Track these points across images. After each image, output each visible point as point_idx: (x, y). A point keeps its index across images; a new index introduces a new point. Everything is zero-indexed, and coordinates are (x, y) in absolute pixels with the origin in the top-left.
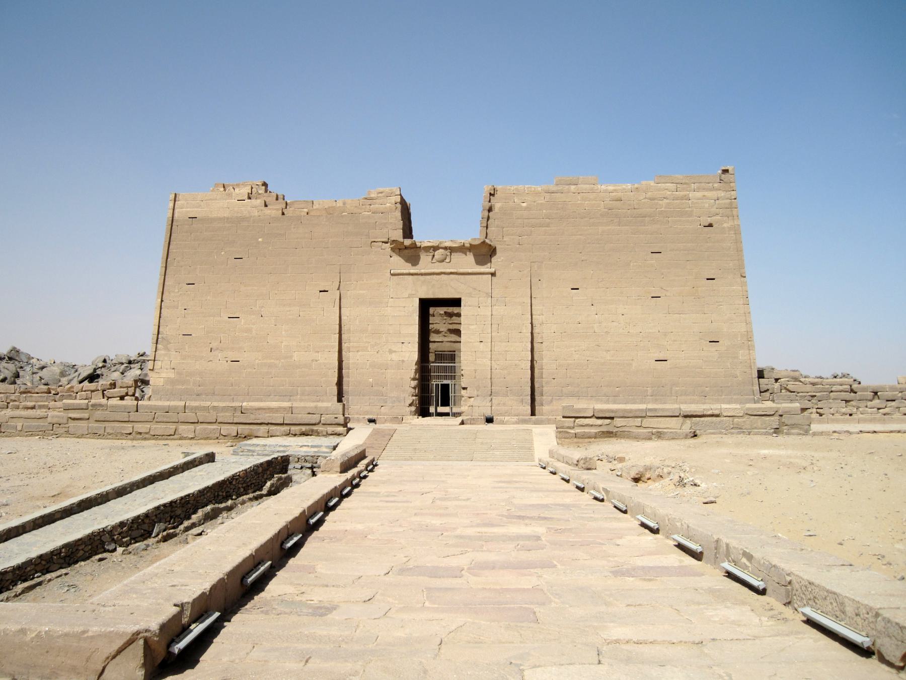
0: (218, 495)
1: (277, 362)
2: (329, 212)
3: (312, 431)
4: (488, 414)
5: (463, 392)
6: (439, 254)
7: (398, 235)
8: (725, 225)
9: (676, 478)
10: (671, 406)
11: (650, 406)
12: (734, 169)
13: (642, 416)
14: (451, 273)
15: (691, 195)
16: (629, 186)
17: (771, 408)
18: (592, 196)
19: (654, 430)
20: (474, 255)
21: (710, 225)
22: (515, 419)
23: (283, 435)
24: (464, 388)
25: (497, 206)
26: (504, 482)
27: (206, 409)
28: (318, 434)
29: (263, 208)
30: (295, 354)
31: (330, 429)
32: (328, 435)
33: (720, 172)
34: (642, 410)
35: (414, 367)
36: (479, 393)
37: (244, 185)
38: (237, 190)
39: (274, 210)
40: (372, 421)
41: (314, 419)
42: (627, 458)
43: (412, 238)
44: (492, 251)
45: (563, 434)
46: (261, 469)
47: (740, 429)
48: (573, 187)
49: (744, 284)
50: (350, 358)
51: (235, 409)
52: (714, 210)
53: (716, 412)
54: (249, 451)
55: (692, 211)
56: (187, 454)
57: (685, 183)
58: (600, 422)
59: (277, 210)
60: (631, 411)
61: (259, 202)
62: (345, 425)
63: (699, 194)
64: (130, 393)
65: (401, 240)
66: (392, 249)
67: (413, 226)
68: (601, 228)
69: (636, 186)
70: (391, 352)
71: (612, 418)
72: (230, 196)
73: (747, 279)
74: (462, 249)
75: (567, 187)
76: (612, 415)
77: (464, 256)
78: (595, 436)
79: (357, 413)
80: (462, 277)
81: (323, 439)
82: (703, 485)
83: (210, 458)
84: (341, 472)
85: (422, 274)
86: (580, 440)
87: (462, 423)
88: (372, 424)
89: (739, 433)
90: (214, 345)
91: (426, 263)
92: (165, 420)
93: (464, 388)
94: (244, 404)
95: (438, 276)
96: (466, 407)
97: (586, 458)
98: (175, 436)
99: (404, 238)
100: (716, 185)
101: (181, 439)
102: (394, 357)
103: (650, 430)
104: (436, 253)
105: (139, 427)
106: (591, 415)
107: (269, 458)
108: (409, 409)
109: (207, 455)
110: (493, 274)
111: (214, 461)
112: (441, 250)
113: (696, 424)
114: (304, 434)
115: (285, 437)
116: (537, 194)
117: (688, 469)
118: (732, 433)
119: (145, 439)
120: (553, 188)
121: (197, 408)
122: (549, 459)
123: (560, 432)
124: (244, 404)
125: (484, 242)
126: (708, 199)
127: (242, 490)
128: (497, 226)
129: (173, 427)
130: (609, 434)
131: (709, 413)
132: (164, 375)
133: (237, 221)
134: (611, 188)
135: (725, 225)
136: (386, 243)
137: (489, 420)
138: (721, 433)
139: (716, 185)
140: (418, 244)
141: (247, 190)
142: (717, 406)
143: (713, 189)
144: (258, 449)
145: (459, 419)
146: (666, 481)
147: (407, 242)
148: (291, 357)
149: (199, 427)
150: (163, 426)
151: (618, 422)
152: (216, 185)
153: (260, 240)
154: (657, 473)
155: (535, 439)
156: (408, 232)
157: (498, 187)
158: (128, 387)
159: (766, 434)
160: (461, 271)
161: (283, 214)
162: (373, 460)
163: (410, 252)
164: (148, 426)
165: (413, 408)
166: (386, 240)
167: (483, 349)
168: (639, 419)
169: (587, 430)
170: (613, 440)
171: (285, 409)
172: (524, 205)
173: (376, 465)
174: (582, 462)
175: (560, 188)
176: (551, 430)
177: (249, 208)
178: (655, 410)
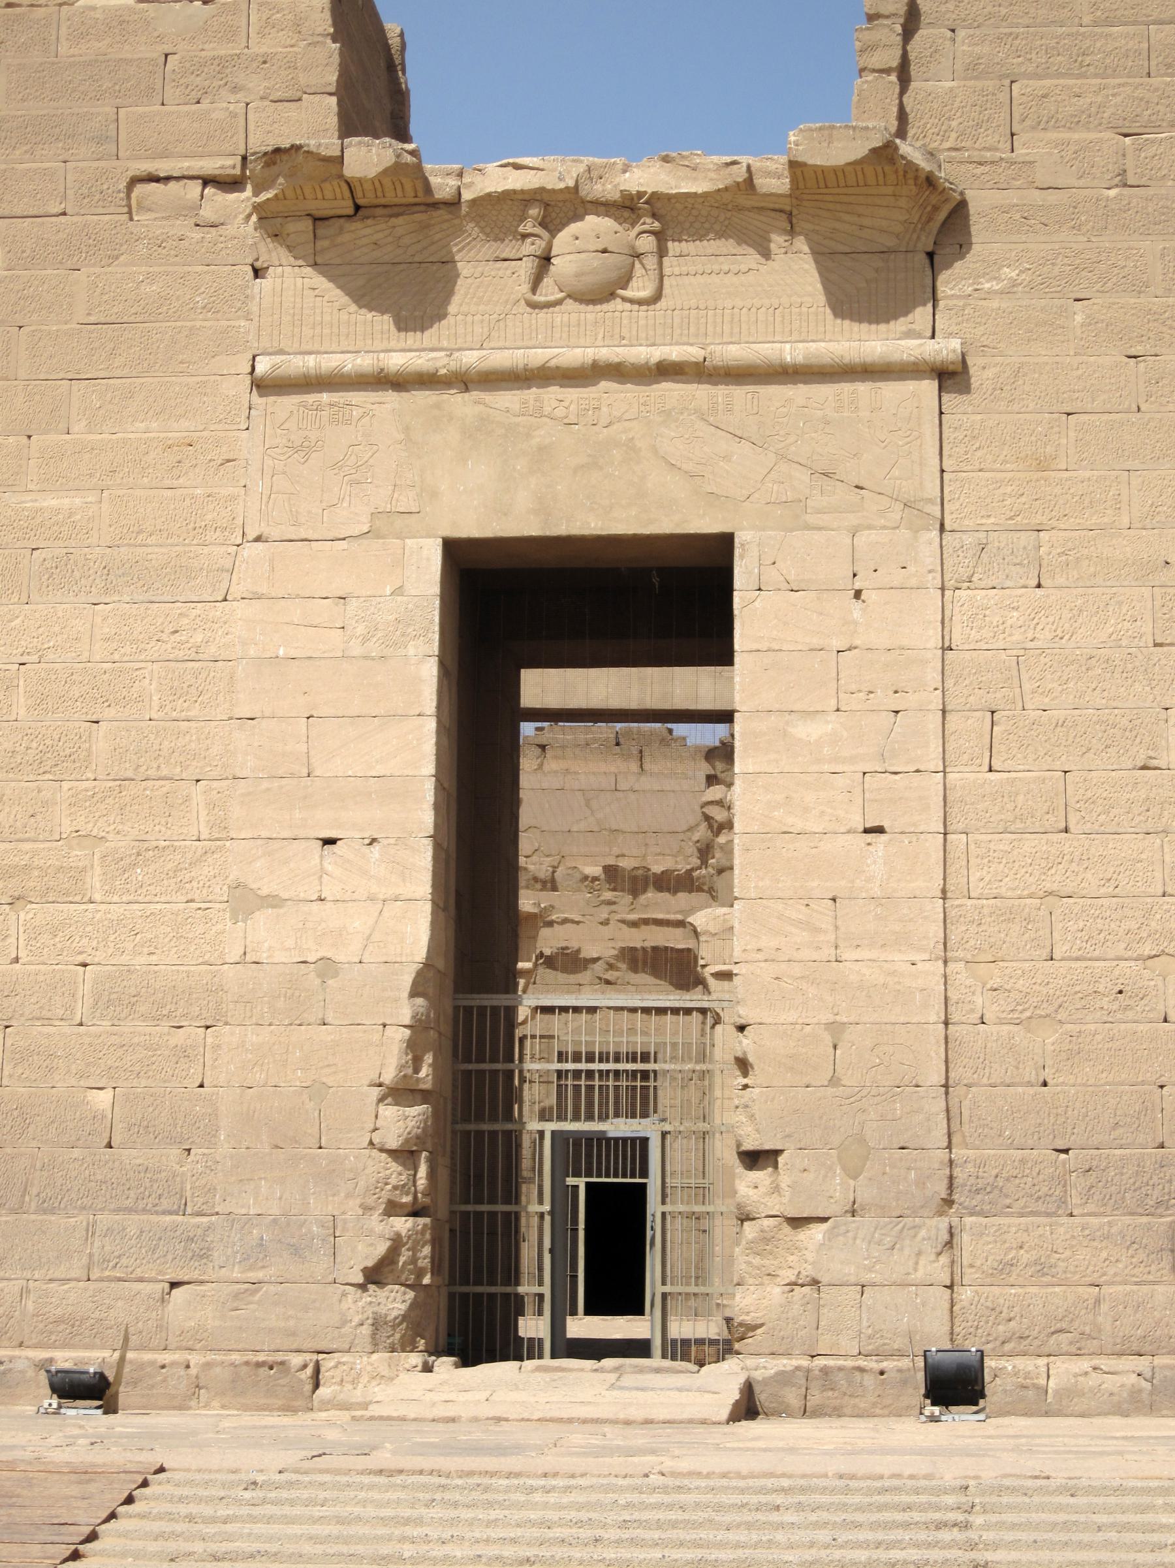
4: (935, 1335)
5: (751, 1186)
6: (581, 245)
7: (314, 123)
14: (666, 371)
20: (823, 256)
22: (1125, 1374)
24: (754, 1159)
35: (405, 1010)
36: (866, 1194)
43: (402, 135)
44: (941, 229)
65: (326, 141)
66: (269, 220)
70: (245, 901)
74: (734, 215)
77: (752, 258)
80: (739, 394)
85: (463, 381)
87: (748, 1408)
88: (84, 1416)
91: (490, 311)
93: (754, 1159)
95: (572, 395)
96: (776, 1292)
102: (269, 936)
104: (563, 239)
108: (363, 1306)
110: (950, 377)
112: (593, 222)
125: (885, 154)
128: (973, 70)
136: (230, 184)
137: (954, 1385)
140: (442, 184)
145: (723, 1381)
147: (368, 157)
156: (375, 91)
160: (734, 353)
163: (375, 228)
165: (394, 1301)
166: (227, 165)
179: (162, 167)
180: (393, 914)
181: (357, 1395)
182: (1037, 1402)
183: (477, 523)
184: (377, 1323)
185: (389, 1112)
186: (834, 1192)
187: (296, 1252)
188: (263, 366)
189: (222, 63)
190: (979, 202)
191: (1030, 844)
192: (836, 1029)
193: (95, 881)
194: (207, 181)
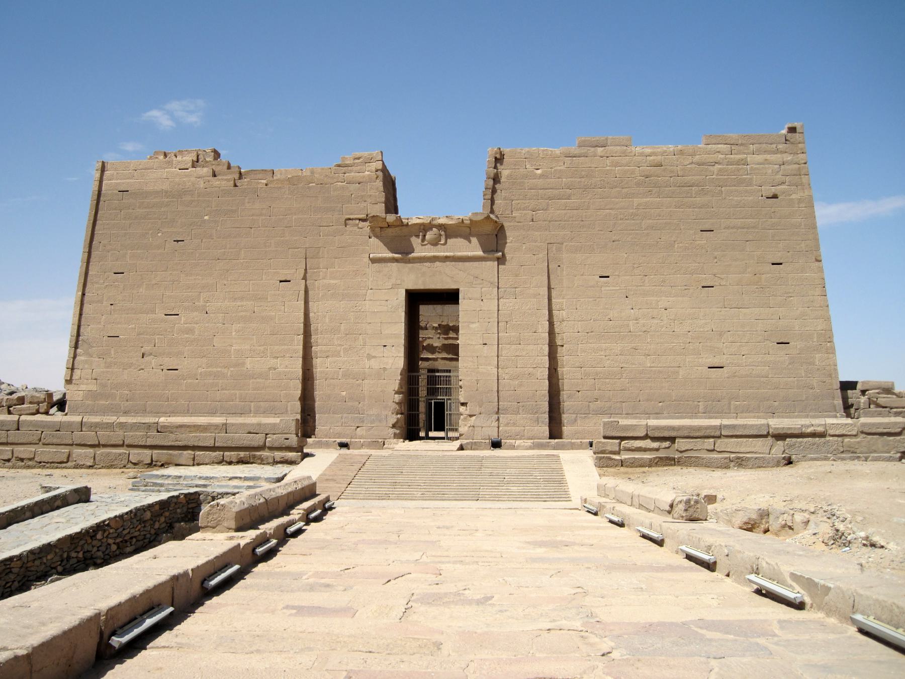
0: (69, 558)
1: (226, 371)
2: (293, 181)
3: (254, 457)
4: (494, 437)
5: (462, 409)
7: (379, 209)
8: (794, 196)
9: (826, 529)
10: (754, 422)
11: (726, 422)
12: (802, 126)
13: (716, 435)
15: (750, 158)
16: (671, 148)
17: (896, 423)
18: (625, 160)
19: (733, 455)
21: (775, 197)
22: (529, 443)
23: (213, 463)
25: (505, 172)
26: (541, 544)
27: (110, 426)
28: (262, 461)
29: (211, 178)
30: (248, 361)
31: (278, 455)
32: (275, 462)
33: (784, 131)
34: (715, 427)
36: (483, 410)
37: (189, 152)
38: (179, 158)
39: (224, 182)
40: (344, 445)
41: (257, 440)
42: (719, 497)
43: (396, 212)
45: (604, 461)
46: (148, 515)
47: (852, 453)
48: (600, 150)
49: (821, 270)
50: (320, 366)
51: (149, 426)
52: (779, 177)
53: (820, 429)
54: (155, 484)
55: (751, 179)
56: (47, 489)
57: (742, 144)
58: (655, 445)
59: (228, 180)
60: (699, 428)
61: (205, 171)
62: (299, 449)
63: (759, 158)
64: (41, 410)
65: (383, 215)
66: (372, 229)
67: (399, 204)
68: (636, 201)
69: (680, 147)
71: (672, 440)
72: (170, 163)
73: (825, 263)
75: (593, 149)
76: (673, 434)
78: (652, 464)
79: (326, 436)
81: (268, 468)
82: (891, 546)
83: (82, 496)
84: (238, 530)
86: (630, 470)
87: (461, 448)
89: (852, 459)
90: (147, 348)
92: (55, 441)
94: (162, 419)
96: (466, 428)
97: (688, 502)
98: (69, 464)
99: (388, 211)
100: (780, 146)
101: (76, 467)
103: (727, 455)
105: (20, 451)
106: (642, 434)
107: (164, 496)
109: (76, 491)
111: (87, 500)
113: (791, 446)
114: (241, 462)
115: (216, 466)
116: (554, 158)
117: (849, 516)
118: (843, 459)
119: (29, 467)
120: (574, 149)
121: (97, 425)
122: (603, 500)
123: (601, 458)
124: (162, 419)
125: (488, 217)
126: (770, 164)
127: (114, 547)
128: (505, 199)
129: (66, 450)
130: (669, 462)
131: (809, 430)
132: (83, 387)
133: (179, 194)
134: (648, 151)
135: (794, 196)
137: (496, 445)
138: (826, 459)
139: (780, 146)
141: (191, 157)
142: (821, 421)
143: (777, 151)
144: (169, 481)
145: (457, 444)
146: (805, 535)
147: (391, 218)
148: (243, 364)
149: (100, 451)
150: (53, 449)
151: (681, 444)
152: (156, 153)
153: (206, 218)
154: (781, 521)
155: (566, 468)
156: (392, 206)
157: (506, 150)
158: (38, 403)
159: (889, 459)
161: (235, 186)
162: (328, 500)
164: (32, 449)
166: (363, 216)
167: (489, 352)
168: (712, 440)
169: (637, 455)
170: (677, 469)
171: (216, 426)
172: (539, 172)
173: (331, 508)
174: (682, 507)
175: (583, 150)
176: (587, 457)
177: (193, 179)
178: (734, 427)
179: (352, 217)
180: (396, 360)
181: (391, 446)
182: (513, 447)
183: (411, 287)
184: (395, 434)
185: (396, 396)
186: (477, 410)
187: (380, 421)
188: (371, 256)
189: (362, 196)
190: (506, 225)
191: (513, 347)
192: (478, 381)
193: (342, 353)
194: (360, 220)
